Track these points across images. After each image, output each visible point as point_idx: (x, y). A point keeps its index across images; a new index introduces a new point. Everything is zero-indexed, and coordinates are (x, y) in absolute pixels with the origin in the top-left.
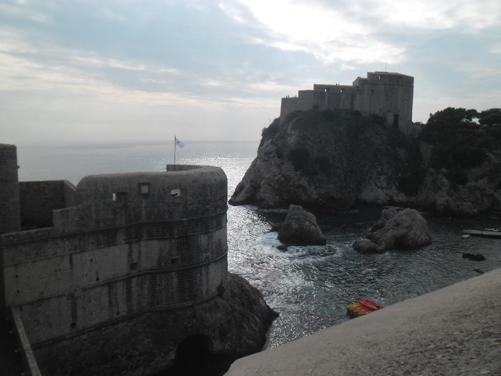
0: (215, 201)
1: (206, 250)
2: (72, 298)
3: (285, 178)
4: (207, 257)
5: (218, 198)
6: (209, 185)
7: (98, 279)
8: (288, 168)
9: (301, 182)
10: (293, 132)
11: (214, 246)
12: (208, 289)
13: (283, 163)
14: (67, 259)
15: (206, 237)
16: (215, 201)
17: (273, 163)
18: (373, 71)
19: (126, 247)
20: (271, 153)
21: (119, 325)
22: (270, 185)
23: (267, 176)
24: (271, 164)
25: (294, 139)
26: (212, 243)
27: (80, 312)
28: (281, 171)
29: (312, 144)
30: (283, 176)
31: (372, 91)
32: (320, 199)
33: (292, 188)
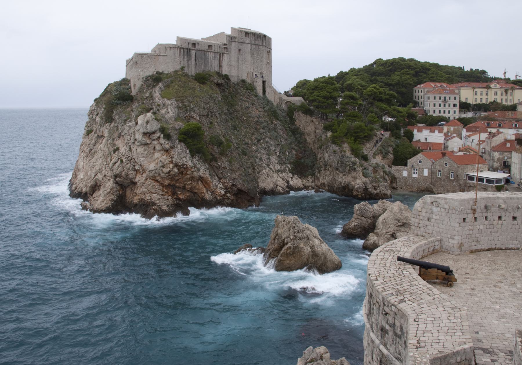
3: (179, 170)
8: (182, 155)
9: (201, 173)
10: (168, 102)
13: (172, 147)
17: (158, 147)
18: (236, 26)
20: (154, 133)
22: (157, 181)
23: (152, 167)
24: (154, 148)
25: (172, 111)
28: (172, 158)
29: (198, 118)
30: (176, 165)
31: (240, 50)
32: (228, 195)
33: (189, 183)
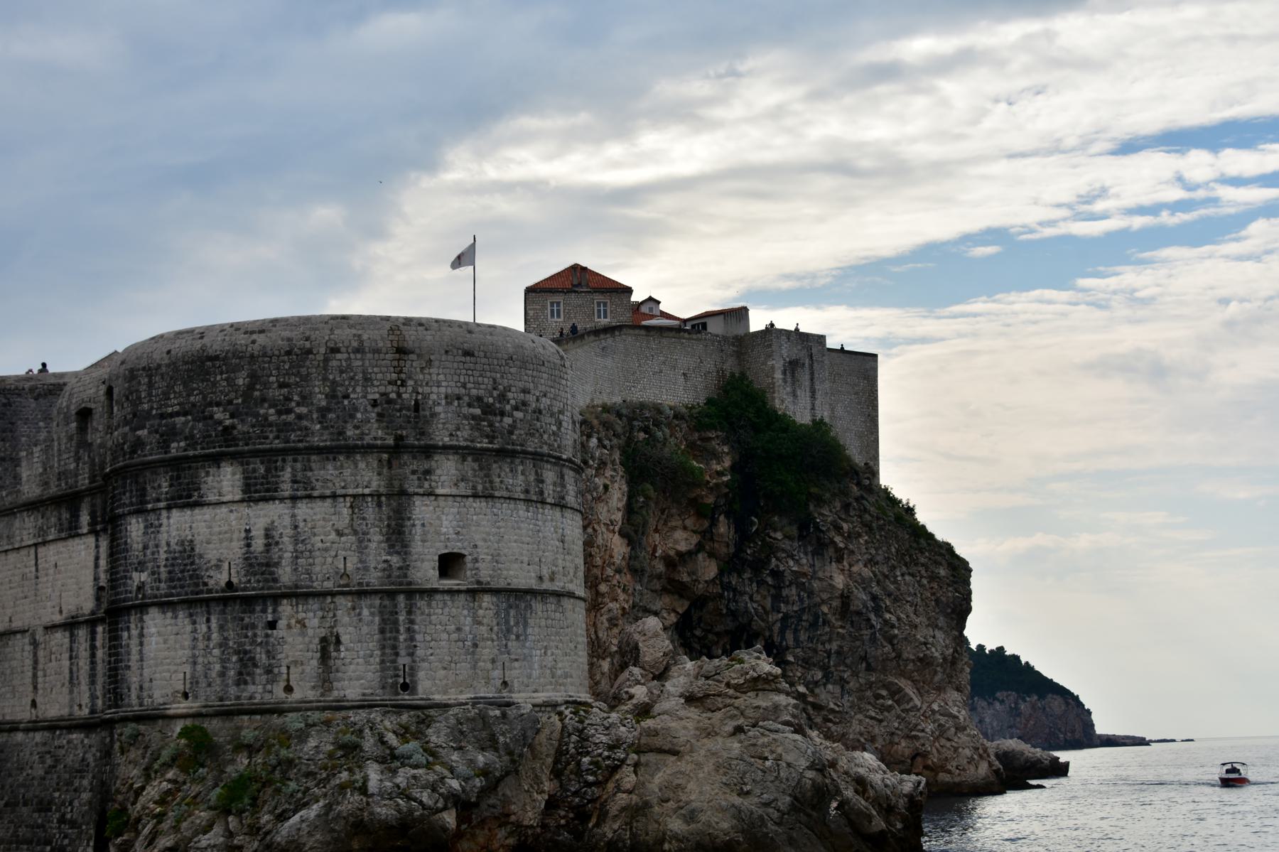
0: (162, 416)
1: (139, 563)
2: (35, 644)
4: (141, 587)
5: (177, 408)
6: (144, 369)
7: (61, 612)
11: (163, 556)
12: (141, 688)
14: (32, 551)
15: (142, 526)
16: (162, 416)
19: (91, 540)
21: (74, 736)
26: (157, 546)
27: (40, 674)
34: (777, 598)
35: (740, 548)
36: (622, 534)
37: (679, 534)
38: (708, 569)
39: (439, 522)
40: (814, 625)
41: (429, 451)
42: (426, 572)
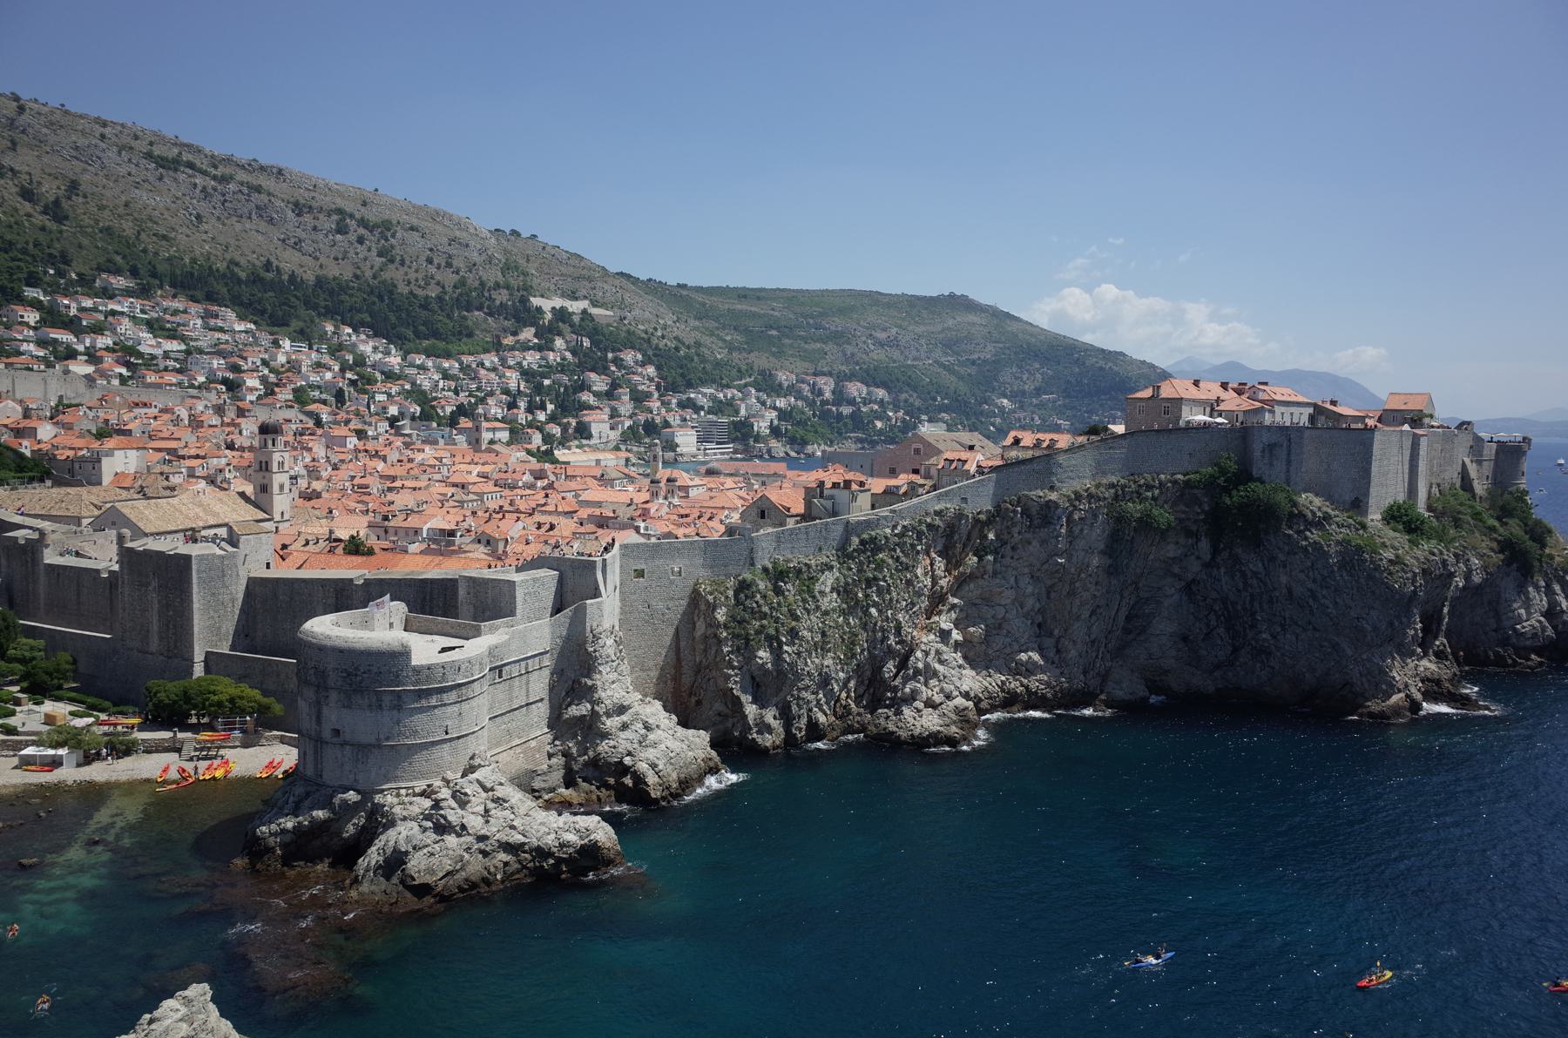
34: (1245, 583)
35: (1213, 558)
36: (1103, 552)
37: (1171, 547)
38: (1195, 567)
39: (333, 715)
40: (1271, 601)
41: (326, 689)
42: (327, 734)
